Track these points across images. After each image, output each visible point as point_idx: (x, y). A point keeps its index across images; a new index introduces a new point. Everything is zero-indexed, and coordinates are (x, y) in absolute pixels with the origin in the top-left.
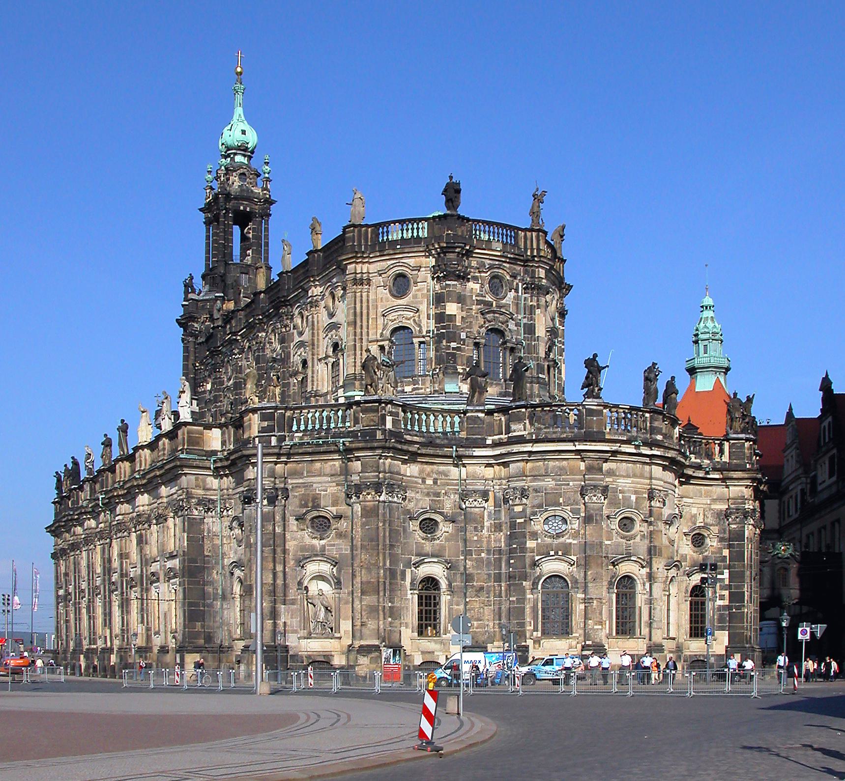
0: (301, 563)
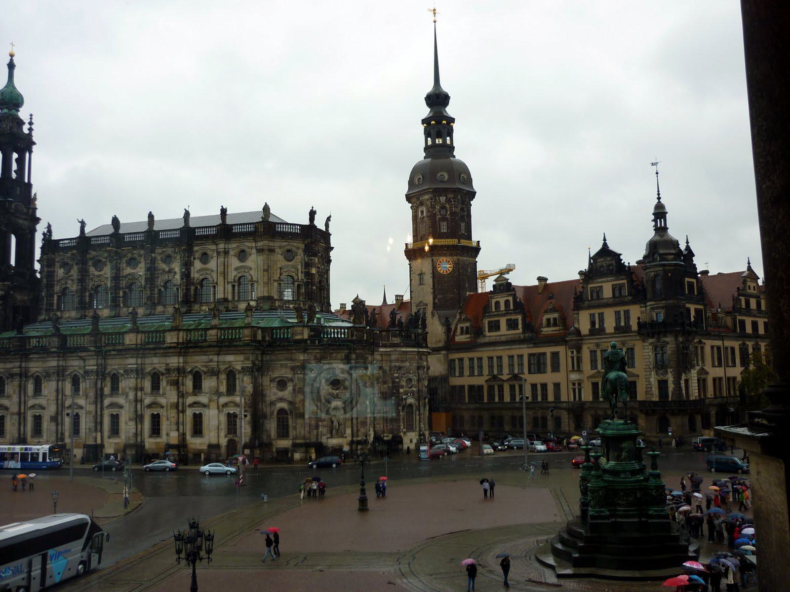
0: (329, 402)
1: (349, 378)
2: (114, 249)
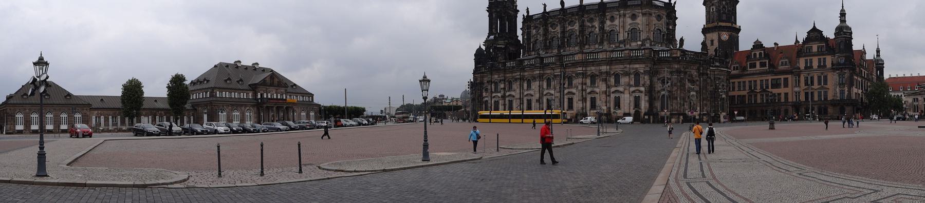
1: (699, 79)
2: (562, 17)
